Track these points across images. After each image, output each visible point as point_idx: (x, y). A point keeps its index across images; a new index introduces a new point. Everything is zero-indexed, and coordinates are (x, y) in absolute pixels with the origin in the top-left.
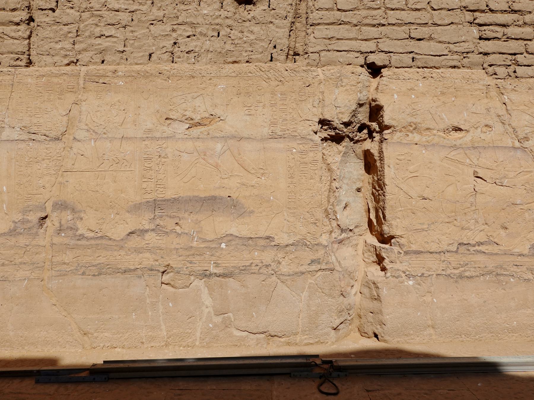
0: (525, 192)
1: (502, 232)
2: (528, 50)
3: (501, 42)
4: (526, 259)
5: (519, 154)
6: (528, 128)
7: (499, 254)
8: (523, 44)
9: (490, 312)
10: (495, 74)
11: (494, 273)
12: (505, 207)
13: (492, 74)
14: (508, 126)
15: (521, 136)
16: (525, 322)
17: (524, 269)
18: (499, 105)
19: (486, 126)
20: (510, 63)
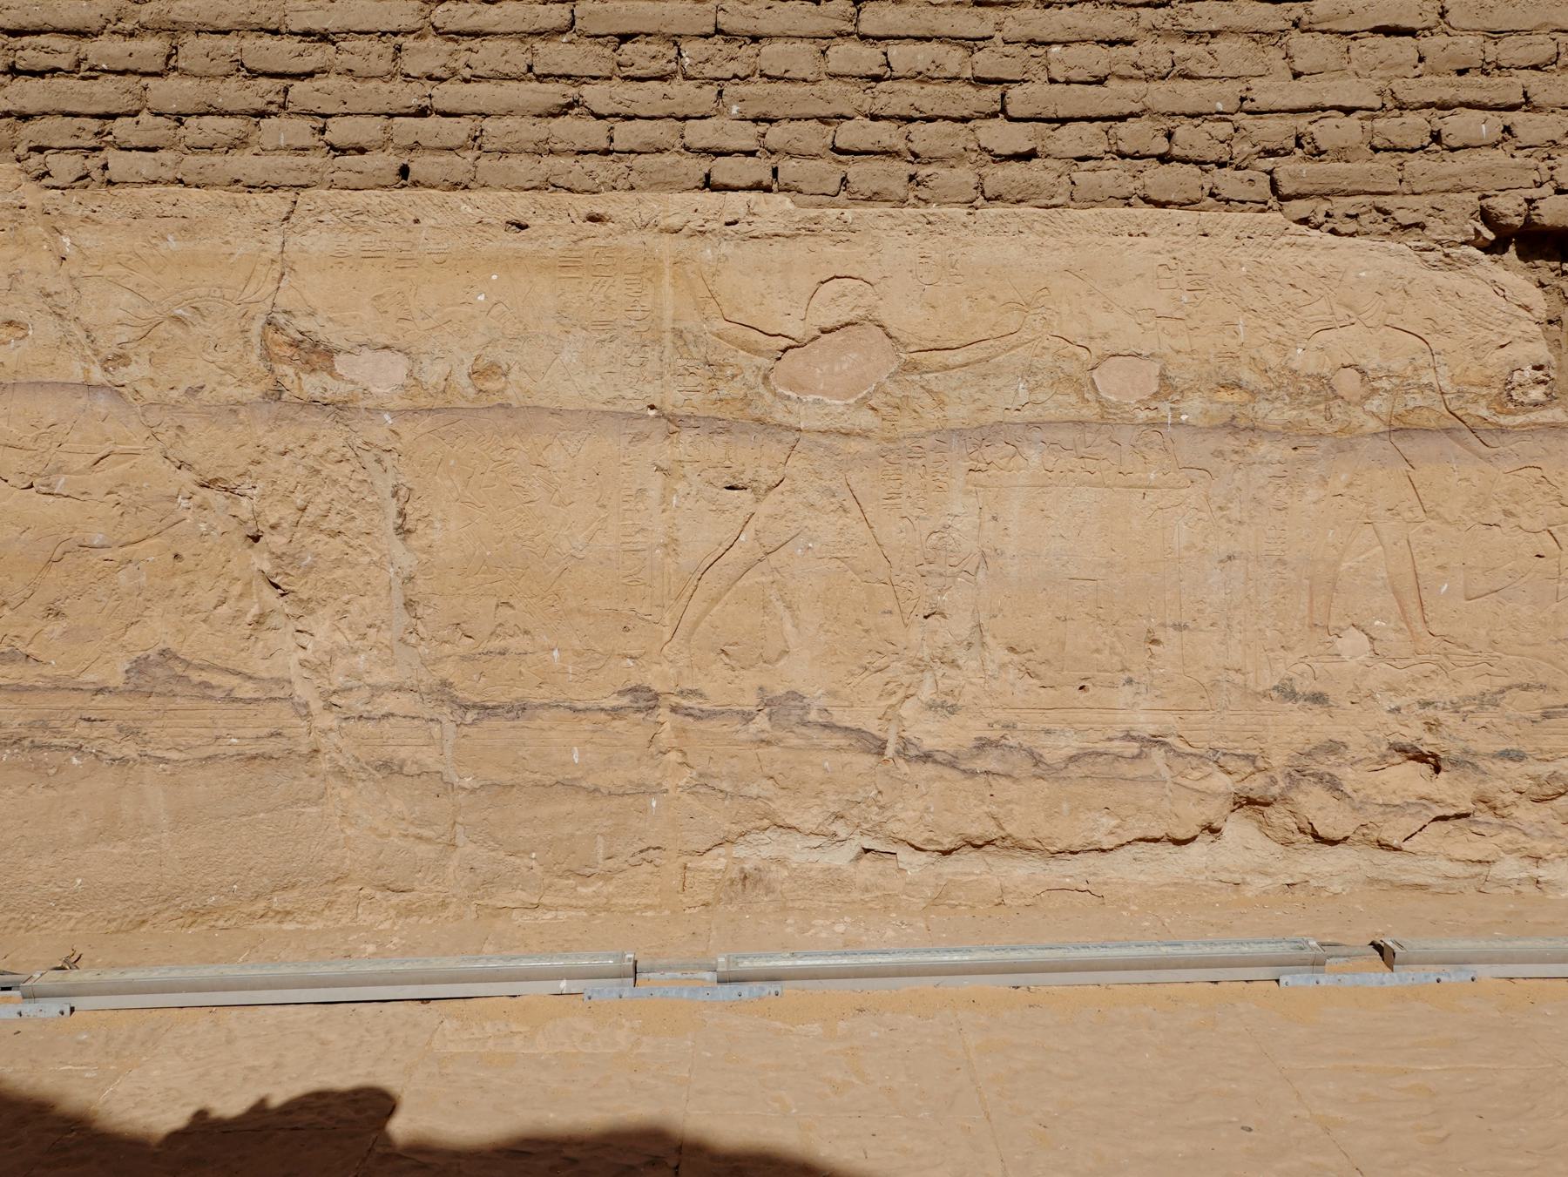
0: (117, 511)
1: (58, 627)
2: (150, 105)
3: (71, 82)
4: (117, 702)
5: (102, 403)
6: (124, 328)
7: (36, 688)
8: (137, 89)
9: (9, 853)
10: (47, 174)
11: (26, 743)
12: (57, 556)
13: (36, 173)
14: (72, 325)
15: (106, 352)
16: (106, 880)
17: (111, 729)
18: (47, 262)
19: (10, 323)
20: (94, 143)
